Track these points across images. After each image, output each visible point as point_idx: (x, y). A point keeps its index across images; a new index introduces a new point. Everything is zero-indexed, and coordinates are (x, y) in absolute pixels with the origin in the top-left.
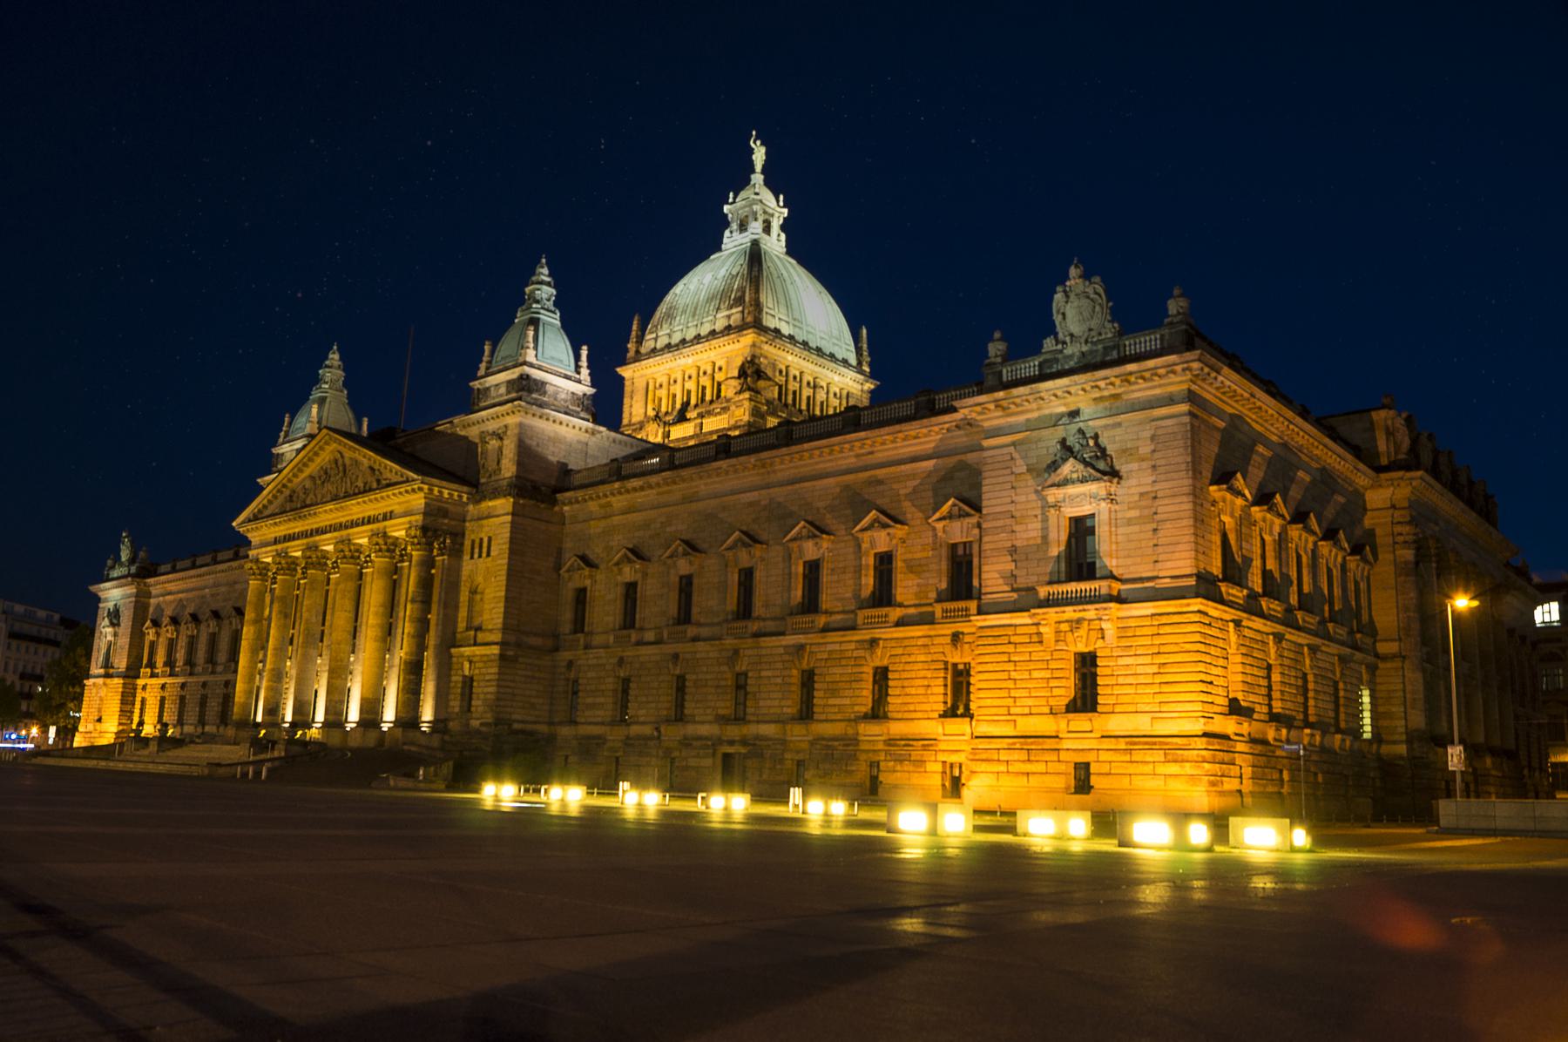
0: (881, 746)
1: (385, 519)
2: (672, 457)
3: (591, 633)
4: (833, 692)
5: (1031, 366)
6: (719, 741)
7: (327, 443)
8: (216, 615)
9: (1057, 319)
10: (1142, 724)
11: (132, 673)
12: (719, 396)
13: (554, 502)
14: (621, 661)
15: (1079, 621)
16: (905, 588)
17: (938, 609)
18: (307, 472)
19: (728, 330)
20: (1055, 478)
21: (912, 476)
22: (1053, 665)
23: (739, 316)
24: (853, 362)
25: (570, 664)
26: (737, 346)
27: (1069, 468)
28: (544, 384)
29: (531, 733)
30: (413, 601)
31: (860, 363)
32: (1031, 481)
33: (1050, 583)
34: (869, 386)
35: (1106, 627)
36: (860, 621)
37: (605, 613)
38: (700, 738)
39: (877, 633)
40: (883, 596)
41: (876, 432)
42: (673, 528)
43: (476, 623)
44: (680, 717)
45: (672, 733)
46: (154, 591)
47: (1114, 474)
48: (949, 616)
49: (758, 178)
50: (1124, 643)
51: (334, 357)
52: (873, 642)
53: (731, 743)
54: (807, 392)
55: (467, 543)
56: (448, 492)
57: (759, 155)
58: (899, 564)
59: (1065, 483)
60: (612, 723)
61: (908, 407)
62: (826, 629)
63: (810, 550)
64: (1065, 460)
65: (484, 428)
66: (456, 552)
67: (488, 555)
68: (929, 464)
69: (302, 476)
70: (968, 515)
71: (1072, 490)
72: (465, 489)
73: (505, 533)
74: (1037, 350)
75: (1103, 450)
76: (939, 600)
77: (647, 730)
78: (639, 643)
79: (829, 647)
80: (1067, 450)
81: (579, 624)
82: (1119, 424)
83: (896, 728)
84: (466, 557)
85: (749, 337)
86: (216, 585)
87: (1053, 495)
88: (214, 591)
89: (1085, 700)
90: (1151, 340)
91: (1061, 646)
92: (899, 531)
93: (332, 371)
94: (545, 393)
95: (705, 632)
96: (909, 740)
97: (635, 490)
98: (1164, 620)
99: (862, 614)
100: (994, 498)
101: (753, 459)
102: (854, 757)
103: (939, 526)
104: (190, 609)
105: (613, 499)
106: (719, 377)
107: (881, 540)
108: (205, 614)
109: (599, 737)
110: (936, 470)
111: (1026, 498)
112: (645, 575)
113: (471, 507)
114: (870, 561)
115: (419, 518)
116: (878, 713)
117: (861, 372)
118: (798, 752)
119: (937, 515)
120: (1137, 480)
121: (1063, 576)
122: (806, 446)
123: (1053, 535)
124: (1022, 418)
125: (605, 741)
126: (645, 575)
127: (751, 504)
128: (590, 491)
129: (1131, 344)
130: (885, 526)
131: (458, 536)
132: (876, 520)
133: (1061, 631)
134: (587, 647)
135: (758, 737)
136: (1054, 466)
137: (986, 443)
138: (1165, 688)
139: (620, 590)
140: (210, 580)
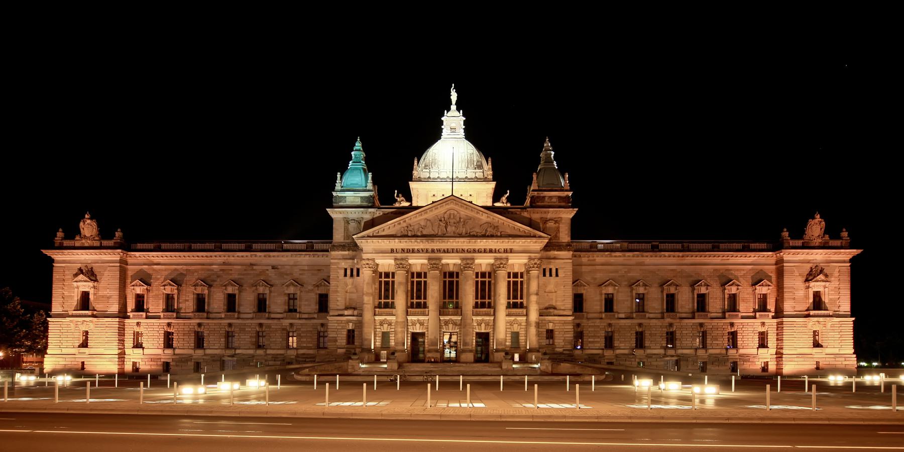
1: (506, 251)
5: (799, 243)
8: (238, 283)
11: (121, 315)
46: (130, 260)
49: (454, 107)
57: (454, 96)
61: (739, 246)
67: (557, 275)
68: (750, 267)
73: (570, 268)
77: (626, 352)
83: (741, 351)
86: (224, 264)
95: (651, 316)
96: (748, 355)
114: (726, 296)
116: (735, 345)
120: (834, 283)
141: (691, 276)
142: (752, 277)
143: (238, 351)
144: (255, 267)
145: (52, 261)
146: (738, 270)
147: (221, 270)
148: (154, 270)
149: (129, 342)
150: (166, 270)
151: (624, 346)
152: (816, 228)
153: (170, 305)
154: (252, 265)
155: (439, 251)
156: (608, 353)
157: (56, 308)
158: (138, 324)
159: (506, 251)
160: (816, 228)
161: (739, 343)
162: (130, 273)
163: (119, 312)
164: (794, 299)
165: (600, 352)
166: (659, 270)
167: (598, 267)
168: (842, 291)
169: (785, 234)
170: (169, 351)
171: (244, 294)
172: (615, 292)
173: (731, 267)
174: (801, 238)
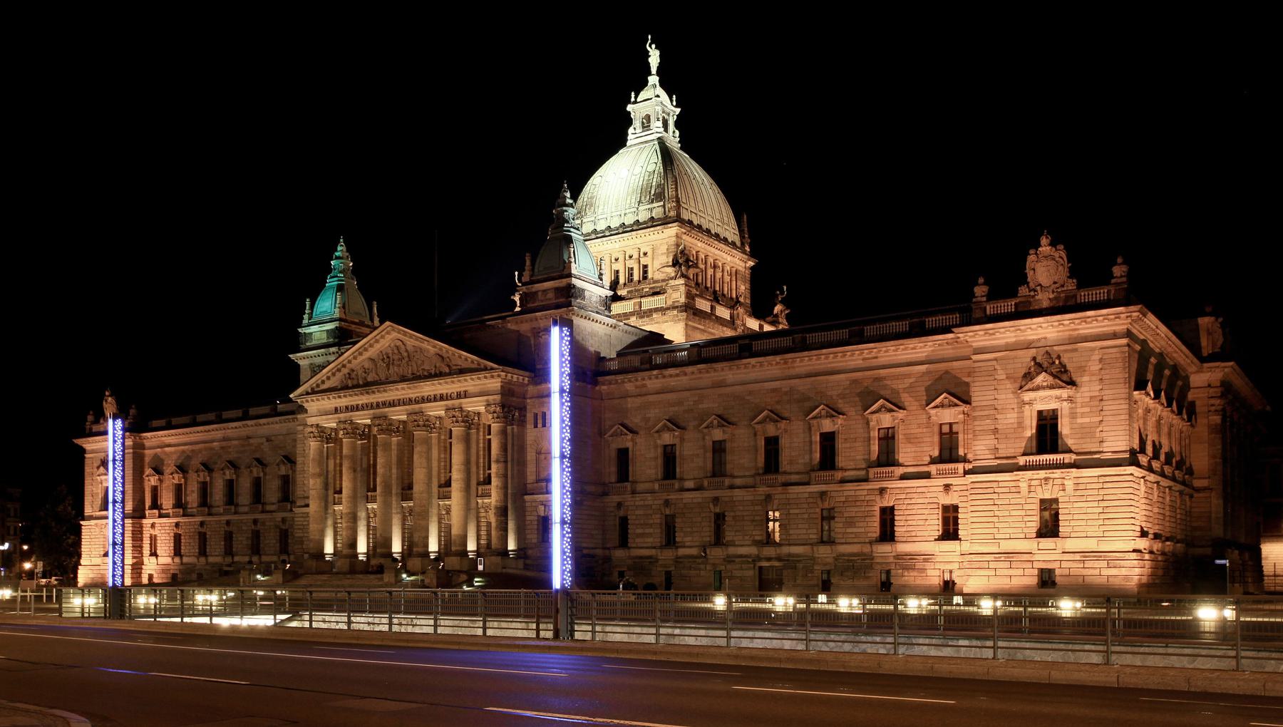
0: (891, 560)
1: (459, 396)
2: (699, 354)
3: (635, 482)
4: (850, 522)
5: (1008, 305)
6: (758, 558)
7: (388, 333)
8: (233, 465)
9: (1030, 274)
10: (1091, 545)
12: (645, 278)
13: (596, 383)
14: (667, 503)
15: (1046, 479)
16: (905, 454)
17: (933, 469)
18: (366, 355)
19: (652, 223)
20: (1030, 385)
21: (908, 376)
22: (1026, 507)
23: (661, 209)
24: (738, 244)
25: (619, 505)
26: (661, 236)
27: (1041, 379)
28: (583, 290)
29: (593, 556)
30: (497, 461)
31: (743, 244)
32: (1009, 385)
33: (1024, 454)
34: (751, 263)
35: (1065, 485)
36: (871, 476)
37: (646, 465)
38: (741, 556)
39: (884, 484)
40: (887, 458)
41: (884, 344)
42: (705, 406)
43: (542, 476)
44: (718, 540)
45: (716, 553)
46: (147, 443)
47: (1072, 383)
48: (941, 474)
50: (1079, 493)
51: (341, 249)
52: (882, 491)
53: (769, 559)
54: (710, 272)
55: (530, 417)
56: (517, 376)
58: (900, 437)
59: (1038, 388)
60: (661, 547)
61: (903, 326)
62: (843, 481)
63: (827, 426)
64: (1038, 374)
65: (535, 324)
66: (522, 423)
68: (923, 368)
69: (360, 358)
70: (956, 405)
71: (1041, 393)
72: (527, 374)
74: (1014, 294)
75: (1064, 367)
76: (933, 461)
77: (694, 551)
78: (682, 490)
79: (846, 493)
80: (1040, 368)
81: (623, 475)
82: (1075, 350)
83: (902, 548)
84: (530, 426)
85: (673, 230)
86: (224, 439)
87: (1027, 396)
88: (224, 444)
89: (1049, 528)
90: (1100, 293)
91: (1032, 495)
92: (901, 414)
93: (340, 260)
94: (584, 299)
96: (912, 556)
97: (671, 376)
98: (1108, 479)
99: (872, 471)
100: (980, 395)
101: (778, 358)
102: (871, 567)
103: (933, 412)
104: (200, 458)
105: (648, 382)
106: (644, 261)
107: (886, 420)
108: (195, 463)
109: (650, 557)
110: (928, 372)
111: (1006, 396)
112: (682, 440)
113: (531, 388)
114: (875, 434)
115: (498, 398)
117: (744, 252)
118: (826, 564)
119: (933, 405)
120: (1088, 387)
121: (1034, 450)
122: (824, 351)
123: (1027, 422)
124: (1002, 342)
125: (657, 560)
126: (682, 440)
127: (774, 390)
128: (630, 376)
129: (1086, 295)
130: (891, 411)
131: (523, 409)
132: (882, 406)
133: (1032, 487)
134: (634, 492)
135: (790, 555)
136: (1028, 376)
137: (975, 357)
138: (1107, 522)
139: (660, 451)
140: (219, 434)
141: (809, 399)
142: (927, 389)
143: (236, 559)
144: (251, 441)
145: (84, 451)
146: (897, 377)
147: (222, 448)
148: (166, 453)
149: (146, 551)
150: (175, 452)
151: (690, 542)
152: (1046, 267)
153: (179, 504)
154: (249, 438)
155: (385, 404)
156: (667, 555)
157: (88, 511)
158: (153, 526)
159: (459, 396)
160: (1046, 267)
161: (899, 530)
162: (147, 460)
163: (134, 510)
164: (996, 431)
165: (653, 552)
166: (750, 393)
167: (651, 398)
168: (1109, 407)
169: (980, 291)
170: (203, 559)
171: (241, 479)
172: (677, 441)
173: (882, 372)
174: (1014, 294)
